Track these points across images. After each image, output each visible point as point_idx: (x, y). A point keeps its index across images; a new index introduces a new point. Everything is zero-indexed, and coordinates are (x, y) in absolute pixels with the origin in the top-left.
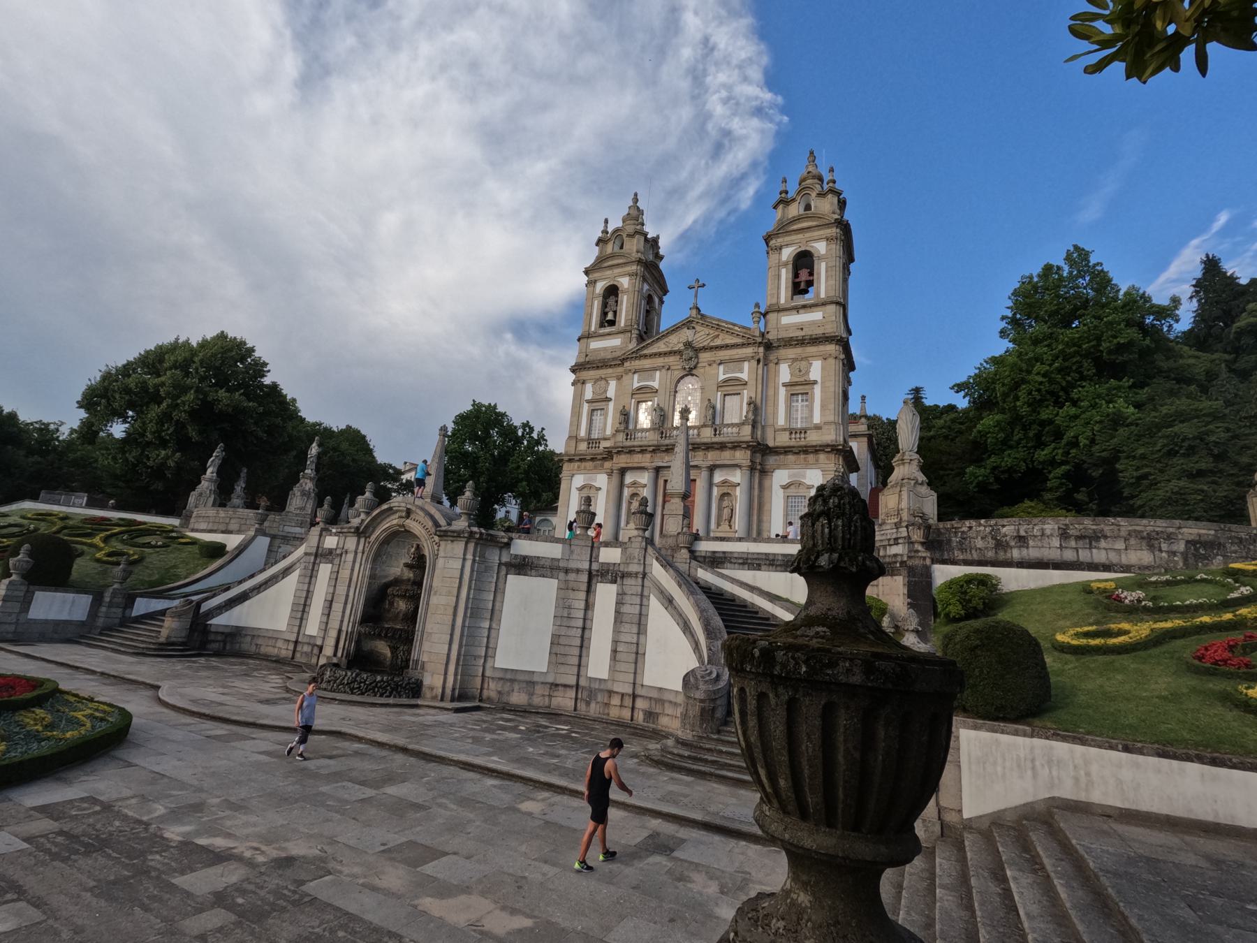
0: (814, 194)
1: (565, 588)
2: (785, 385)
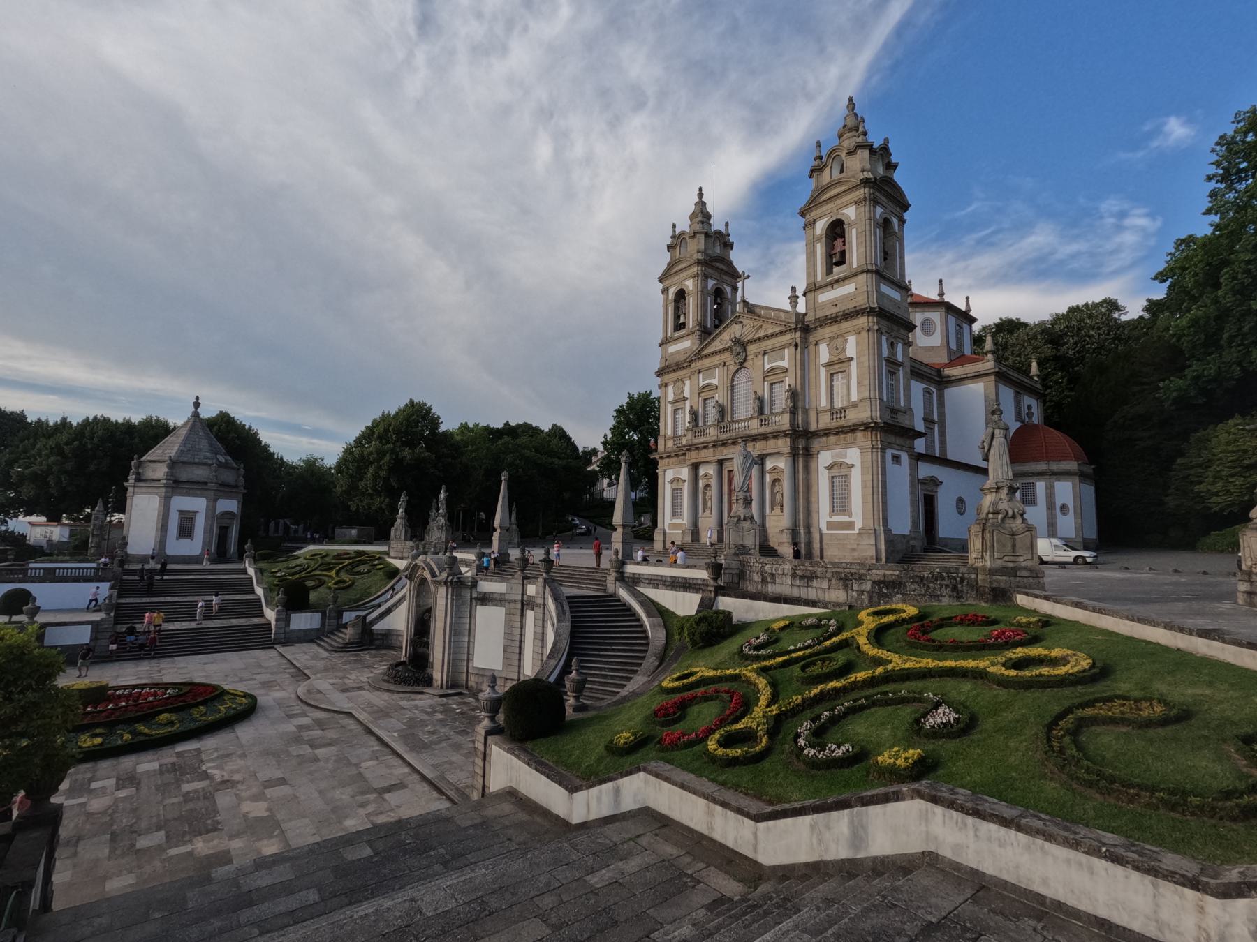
0: (843, 155)
1: (509, 614)
2: (825, 365)
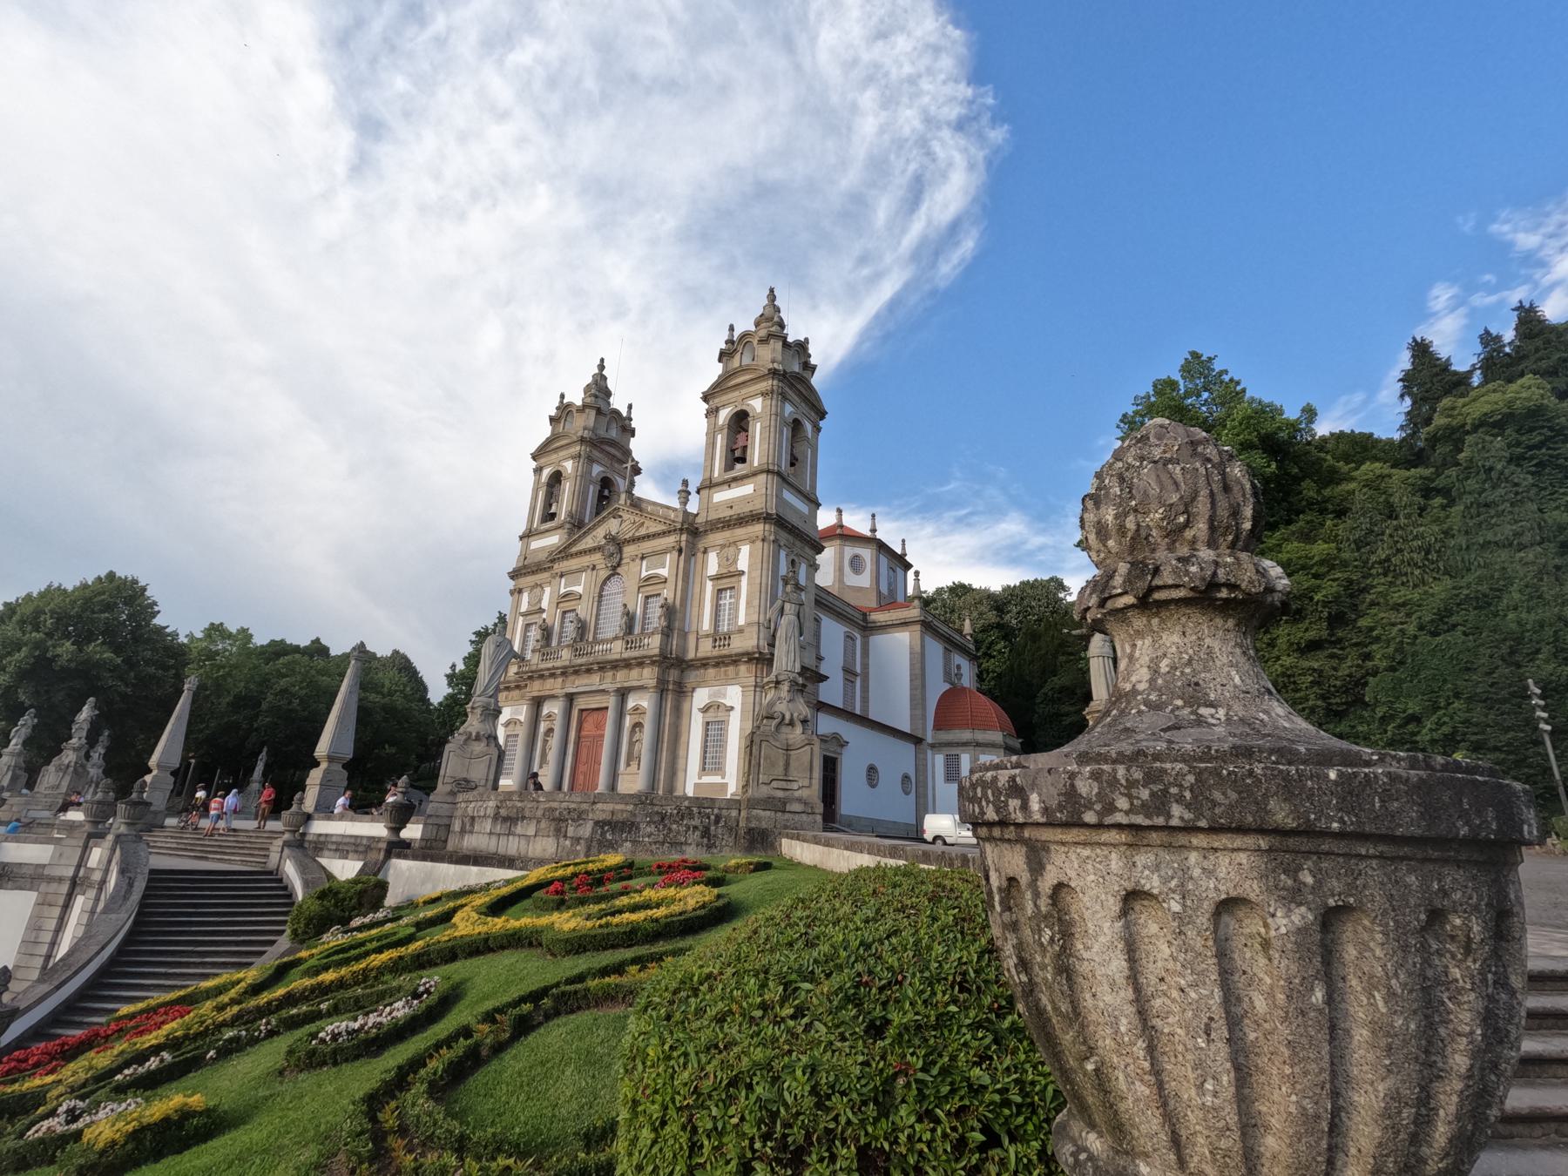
0: (755, 342)
1: (42, 903)
